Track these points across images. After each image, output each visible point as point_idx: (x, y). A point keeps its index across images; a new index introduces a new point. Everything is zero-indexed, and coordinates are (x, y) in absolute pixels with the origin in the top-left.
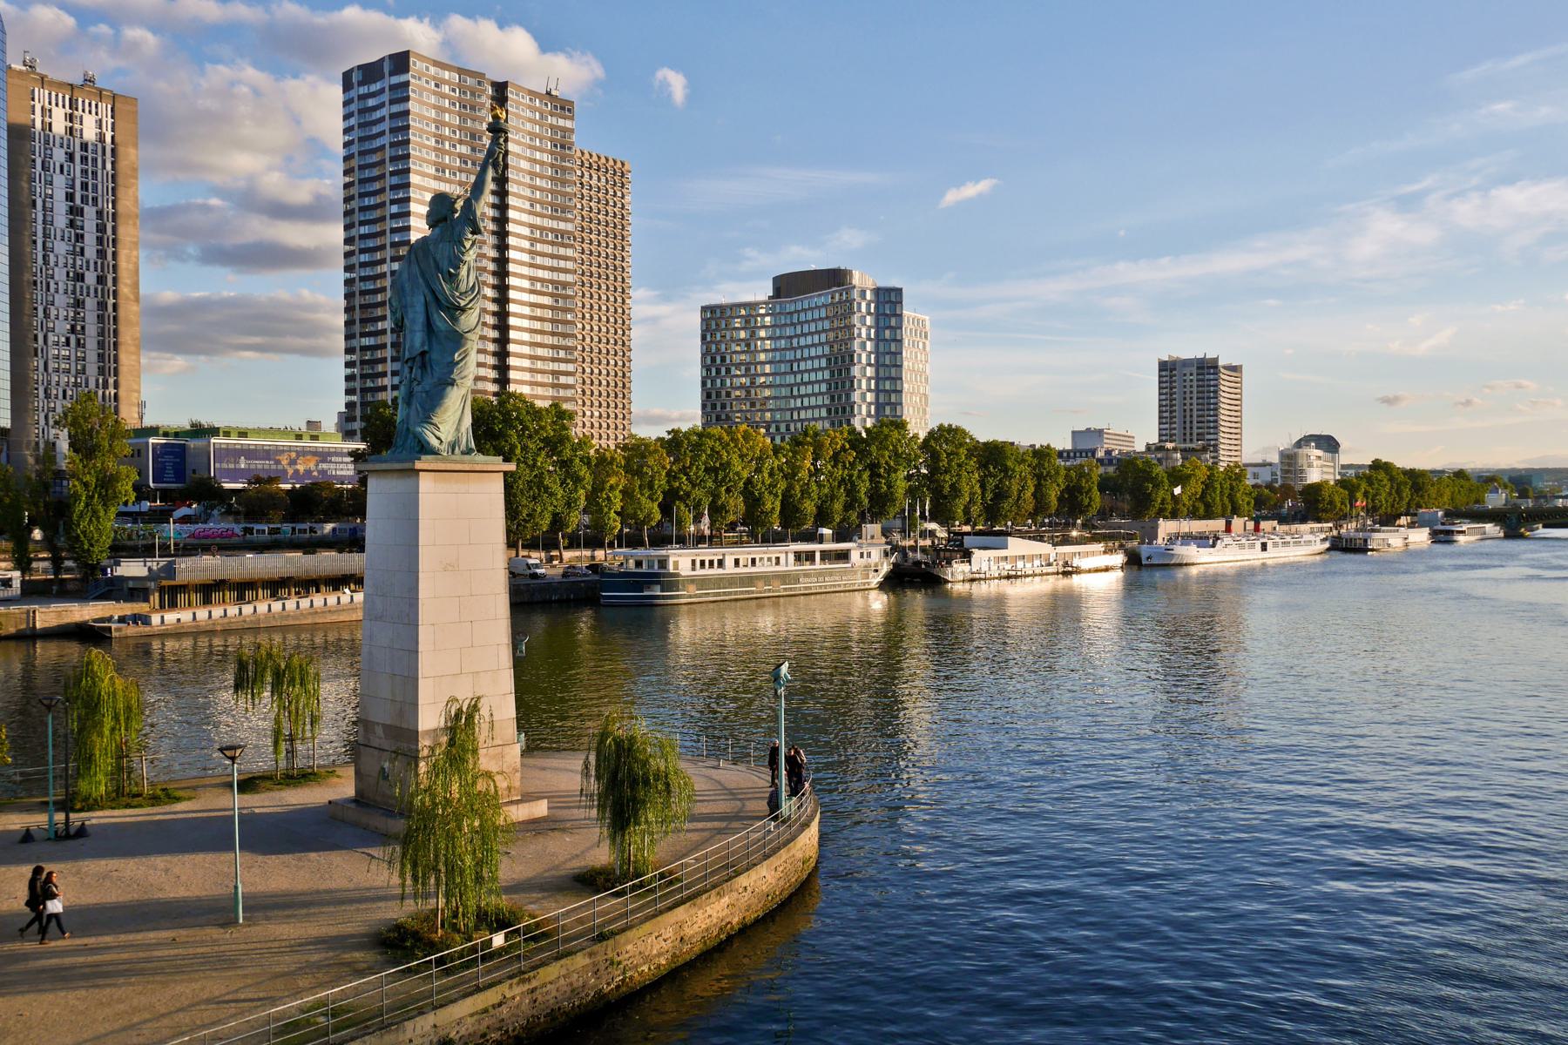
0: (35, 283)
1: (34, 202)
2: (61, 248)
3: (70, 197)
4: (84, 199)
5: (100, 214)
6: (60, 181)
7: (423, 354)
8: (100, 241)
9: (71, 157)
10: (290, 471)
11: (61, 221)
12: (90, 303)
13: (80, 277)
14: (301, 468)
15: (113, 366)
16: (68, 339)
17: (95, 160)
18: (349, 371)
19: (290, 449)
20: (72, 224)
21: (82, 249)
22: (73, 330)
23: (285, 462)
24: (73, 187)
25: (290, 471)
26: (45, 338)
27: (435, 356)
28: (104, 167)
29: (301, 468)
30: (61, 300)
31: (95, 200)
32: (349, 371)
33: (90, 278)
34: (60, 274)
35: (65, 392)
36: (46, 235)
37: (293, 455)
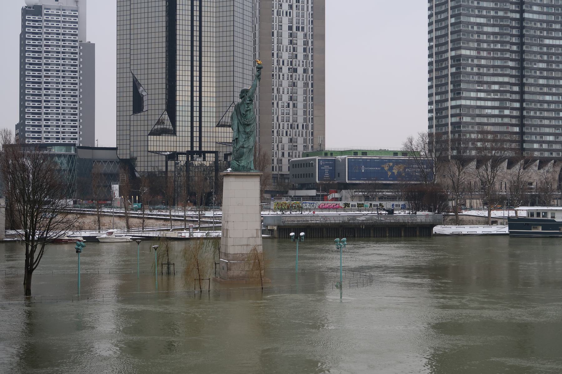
0: (273, 75)
1: (273, 33)
2: (285, 56)
3: (290, 28)
4: (298, 29)
5: (305, 35)
6: (285, 20)
7: (237, 139)
8: (305, 50)
9: (291, 7)
10: (389, 173)
11: (286, 41)
12: (300, 84)
13: (295, 70)
14: (395, 171)
15: (311, 117)
16: (289, 104)
17: (303, 7)
18: (430, 115)
19: (390, 161)
20: (291, 42)
21: (296, 55)
22: (291, 99)
23: (386, 168)
24: (292, 23)
25: (389, 173)
26: (277, 103)
27: (240, 139)
28: (308, 10)
29: (395, 171)
30: (285, 83)
31: (303, 28)
32: (430, 115)
33: (300, 70)
34: (285, 69)
35: (287, 132)
36: (279, 49)
37: (391, 164)
